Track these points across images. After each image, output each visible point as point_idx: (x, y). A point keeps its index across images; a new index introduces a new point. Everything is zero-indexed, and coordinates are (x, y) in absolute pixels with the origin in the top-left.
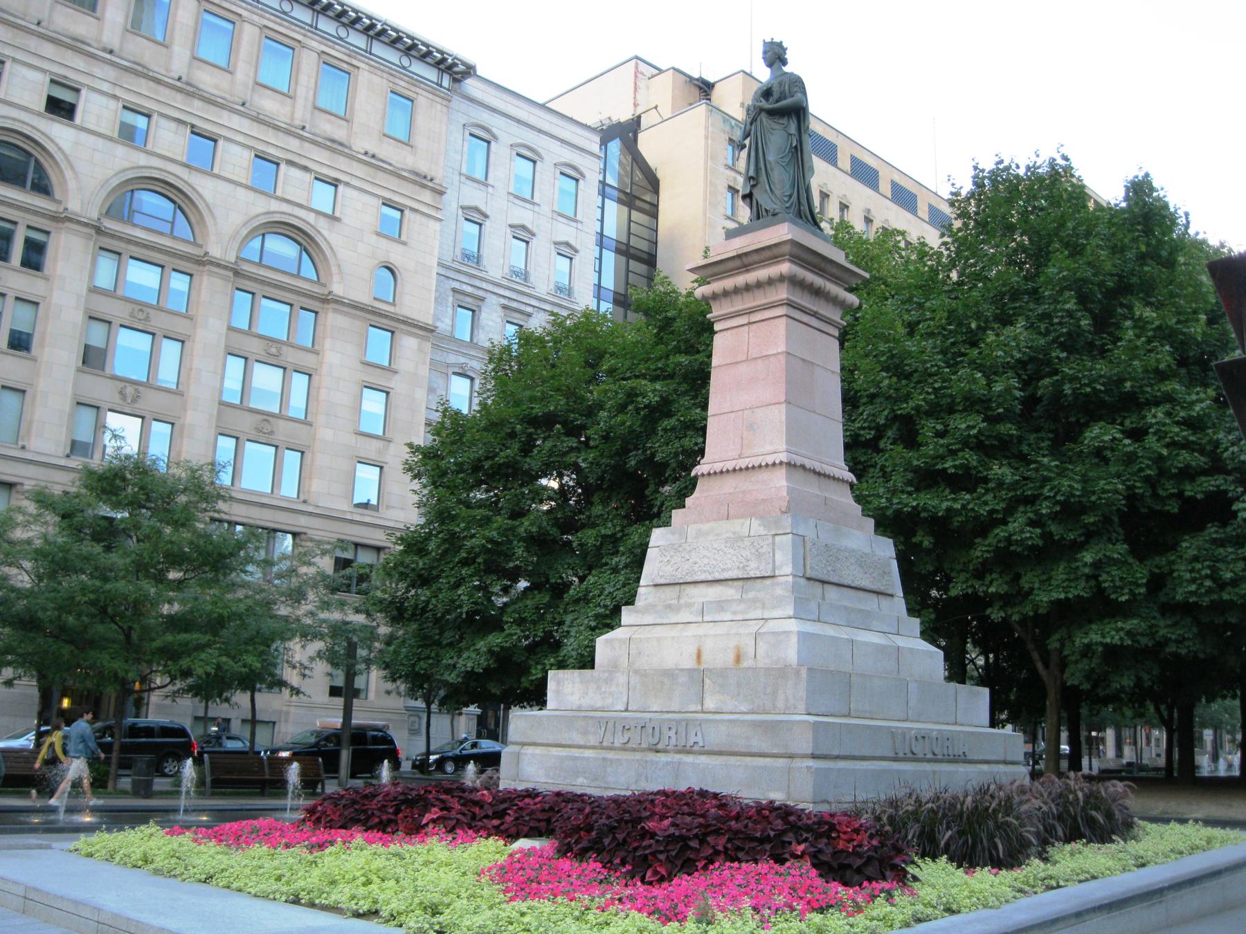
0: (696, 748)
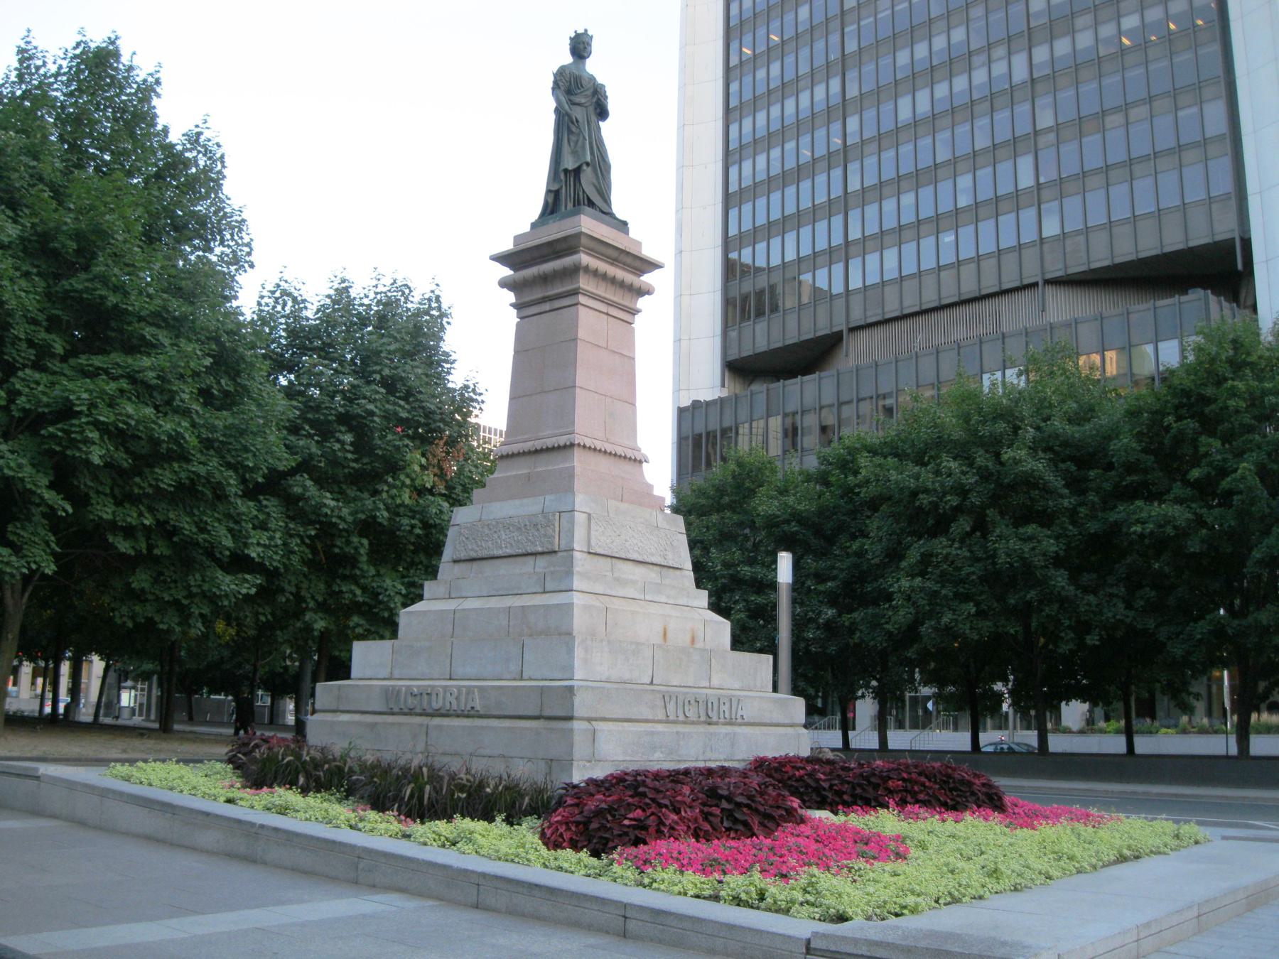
0: (739, 720)
